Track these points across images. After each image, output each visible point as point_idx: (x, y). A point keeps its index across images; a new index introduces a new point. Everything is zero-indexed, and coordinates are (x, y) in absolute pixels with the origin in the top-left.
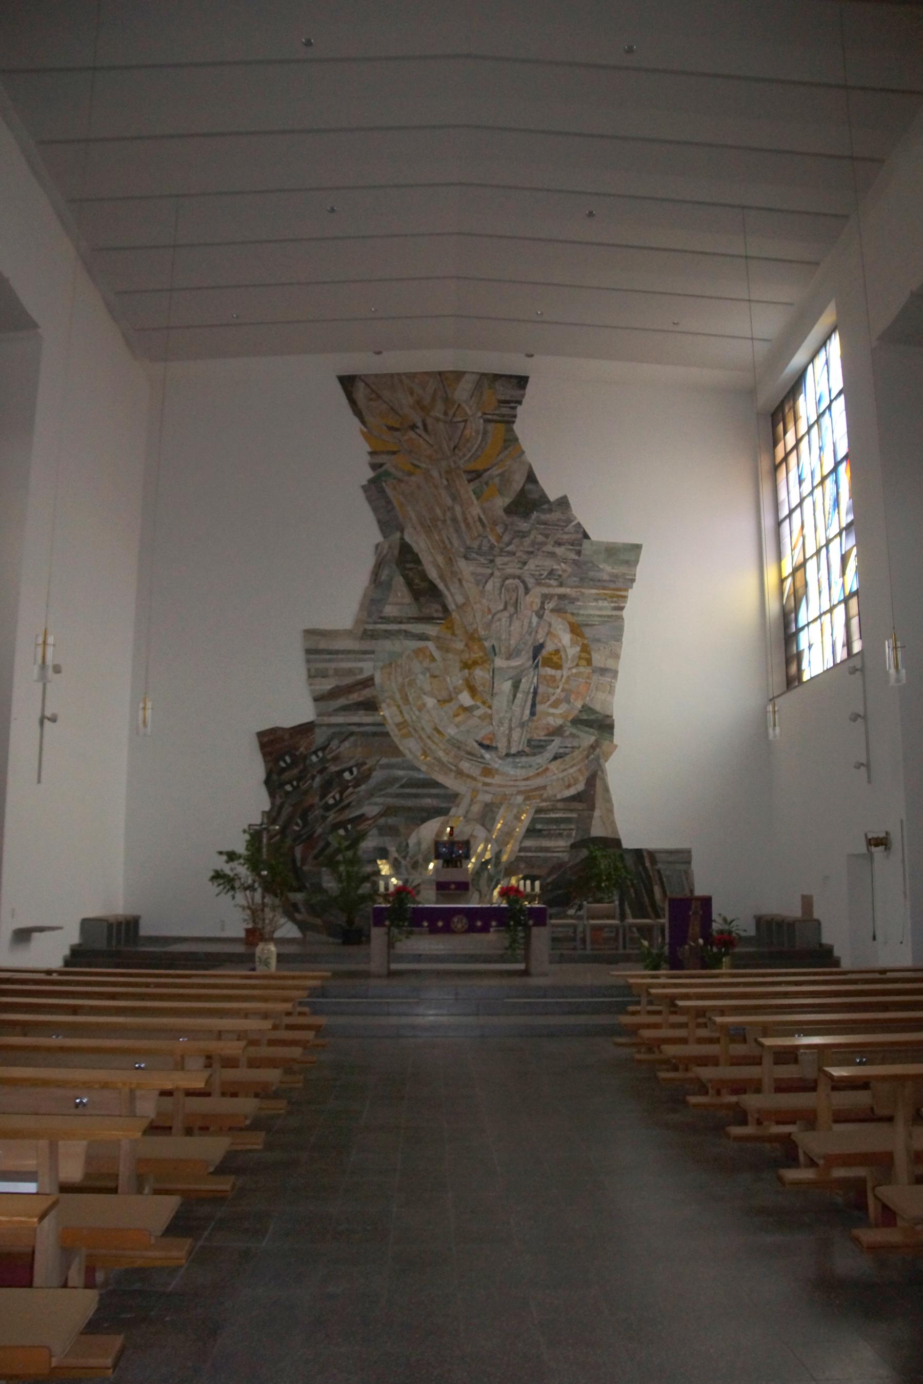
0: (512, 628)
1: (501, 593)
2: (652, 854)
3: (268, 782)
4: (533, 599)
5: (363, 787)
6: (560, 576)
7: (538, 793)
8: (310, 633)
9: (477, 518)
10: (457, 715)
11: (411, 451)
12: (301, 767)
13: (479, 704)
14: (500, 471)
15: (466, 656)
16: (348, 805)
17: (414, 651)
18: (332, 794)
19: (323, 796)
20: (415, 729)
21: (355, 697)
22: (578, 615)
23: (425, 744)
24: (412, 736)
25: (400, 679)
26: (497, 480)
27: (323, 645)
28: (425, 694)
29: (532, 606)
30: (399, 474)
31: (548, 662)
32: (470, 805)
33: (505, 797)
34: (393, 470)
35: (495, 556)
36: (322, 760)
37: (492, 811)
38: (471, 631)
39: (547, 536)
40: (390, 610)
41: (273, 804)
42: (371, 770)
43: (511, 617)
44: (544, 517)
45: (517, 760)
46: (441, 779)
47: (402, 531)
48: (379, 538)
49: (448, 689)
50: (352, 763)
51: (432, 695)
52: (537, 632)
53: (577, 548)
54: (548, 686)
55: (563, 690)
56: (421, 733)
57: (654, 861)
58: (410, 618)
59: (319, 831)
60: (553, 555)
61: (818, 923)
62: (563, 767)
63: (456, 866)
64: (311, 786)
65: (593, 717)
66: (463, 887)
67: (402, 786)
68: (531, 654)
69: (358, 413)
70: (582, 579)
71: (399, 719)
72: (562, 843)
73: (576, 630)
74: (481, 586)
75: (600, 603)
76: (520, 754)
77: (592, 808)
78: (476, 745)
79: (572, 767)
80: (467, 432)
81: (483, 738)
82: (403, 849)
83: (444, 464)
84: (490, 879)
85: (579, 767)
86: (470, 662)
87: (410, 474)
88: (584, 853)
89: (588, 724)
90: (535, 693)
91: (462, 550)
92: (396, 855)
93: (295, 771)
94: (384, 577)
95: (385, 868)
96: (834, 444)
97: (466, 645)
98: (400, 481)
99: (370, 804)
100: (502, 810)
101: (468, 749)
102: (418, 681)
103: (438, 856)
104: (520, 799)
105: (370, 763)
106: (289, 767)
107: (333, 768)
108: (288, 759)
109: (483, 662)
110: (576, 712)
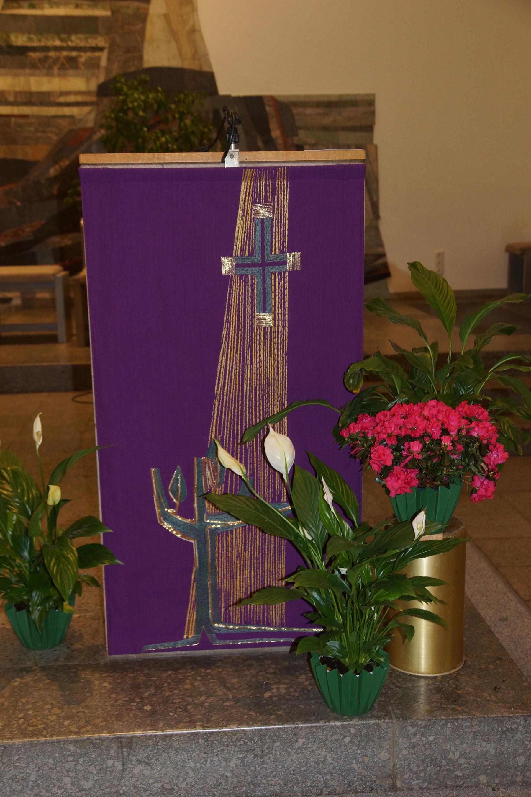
72: (77, 83)
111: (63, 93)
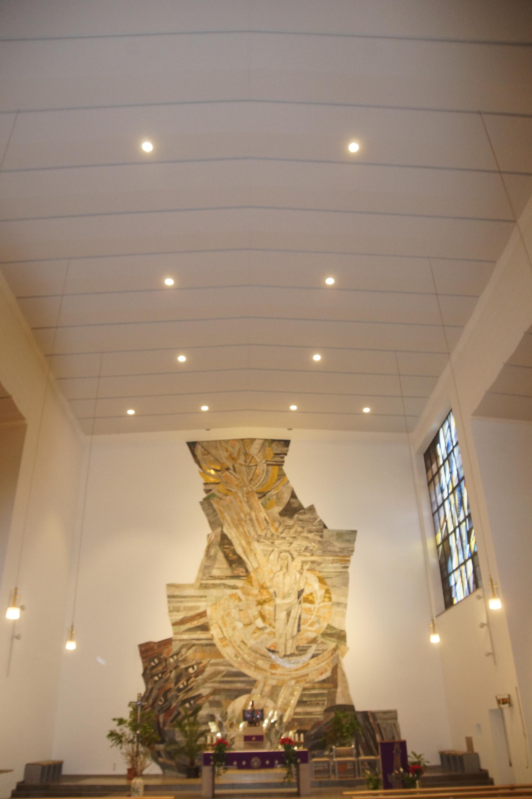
0: (285, 581)
1: (278, 561)
2: (373, 714)
3: (144, 675)
4: (297, 564)
5: (200, 677)
6: (312, 550)
7: (302, 679)
8: (169, 586)
9: (264, 519)
10: (254, 633)
11: (227, 483)
12: (164, 665)
13: (267, 626)
14: (276, 492)
15: (259, 598)
16: (191, 689)
18: (182, 682)
19: (176, 683)
20: (230, 642)
21: (195, 623)
22: (323, 572)
23: (237, 651)
25: (222, 613)
26: (275, 497)
27: (177, 593)
30: (220, 495)
31: (306, 600)
33: (284, 682)
34: (216, 493)
35: (274, 540)
36: (177, 661)
39: (303, 528)
40: (215, 572)
41: (147, 688)
42: (205, 667)
43: (284, 574)
44: (301, 517)
46: (246, 671)
47: (222, 527)
48: (209, 530)
50: (194, 663)
51: (240, 620)
52: (299, 583)
53: (321, 534)
54: (307, 613)
55: (316, 616)
57: (375, 719)
58: (227, 577)
59: (174, 705)
60: (307, 538)
62: (317, 662)
63: (255, 725)
64: (169, 678)
65: (334, 631)
66: (260, 738)
67: (224, 676)
69: (198, 462)
70: (324, 552)
71: (221, 636)
73: (321, 580)
75: (335, 565)
76: (292, 655)
77: (336, 686)
78: (266, 651)
80: (257, 471)
81: (270, 646)
82: (224, 716)
83: (245, 489)
86: (261, 601)
87: (226, 495)
88: (332, 715)
89: (331, 635)
90: (300, 618)
91: (256, 537)
93: (160, 668)
94: (212, 553)
95: (213, 727)
96: (457, 470)
97: (260, 591)
98: (221, 499)
99: (204, 688)
100: (282, 689)
101: (262, 653)
103: (245, 719)
104: (293, 682)
105: (204, 662)
106: (157, 665)
107: (183, 666)
108: (156, 661)
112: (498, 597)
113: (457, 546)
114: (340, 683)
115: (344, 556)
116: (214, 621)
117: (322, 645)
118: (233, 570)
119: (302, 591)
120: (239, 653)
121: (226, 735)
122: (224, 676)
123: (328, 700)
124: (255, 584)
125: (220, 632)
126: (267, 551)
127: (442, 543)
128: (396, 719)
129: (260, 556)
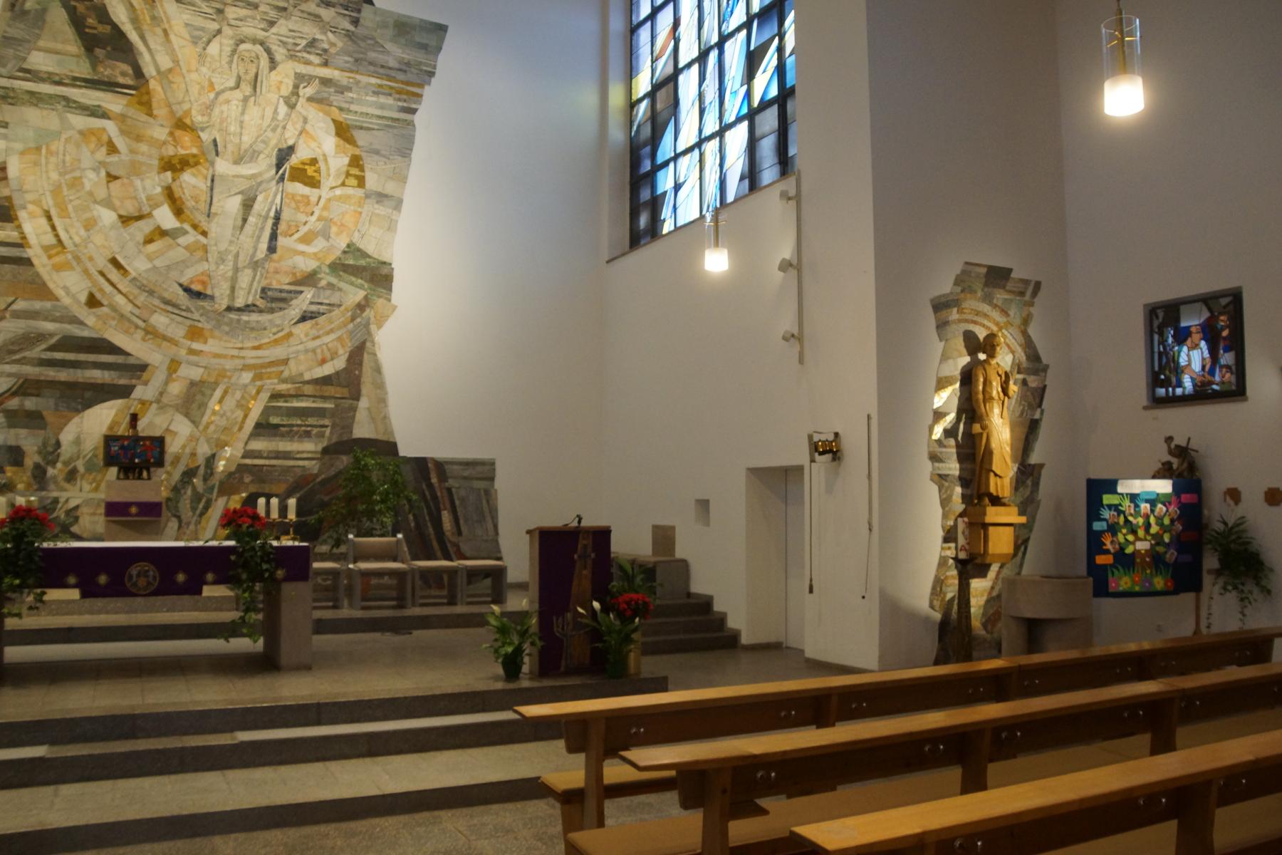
0: (246, 118)
1: (231, 62)
2: (440, 465)
6: (325, 51)
10: (149, 241)
13: (187, 227)
15: (170, 151)
17: (81, 133)
20: (77, 258)
24: (72, 268)
25: (54, 176)
28: (95, 202)
29: (279, 89)
31: (300, 175)
32: (166, 383)
33: (222, 374)
35: (226, 4)
37: (203, 394)
38: (179, 114)
43: (245, 100)
45: (245, 318)
46: (119, 339)
49: (135, 198)
51: (107, 203)
52: (284, 128)
55: (319, 219)
56: (89, 265)
57: (443, 476)
60: (316, 17)
61: (684, 564)
62: (314, 332)
63: (140, 477)
65: (362, 262)
66: (151, 510)
67: (52, 348)
68: (274, 161)
72: (309, 446)
73: (343, 132)
74: (201, 45)
75: (382, 99)
77: (356, 396)
78: (181, 292)
79: (328, 333)
82: (51, 452)
84: (197, 497)
85: (339, 333)
86: (175, 161)
89: (355, 271)
90: (277, 219)
92: (37, 459)
97: (171, 134)
100: (218, 393)
101: (166, 295)
102: (85, 181)
103: (110, 460)
104: (247, 377)
109: (197, 164)
110: (338, 253)
111: (299, 452)
112: (723, 246)
113: (701, 96)
114: (366, 389)
115: (409, 83)
116: (29, 197)
117: (328, 292)
118: (94, 63)
119: (291, 149)
120: (101, 290)
121: (56, 501)
122: (52, 348)
123: (334, 426)
124: (160, 111)
125: (49, 229)
126: (202, 29)
127: (652, 95)
128: (492, 479)
129: (180, 40)
